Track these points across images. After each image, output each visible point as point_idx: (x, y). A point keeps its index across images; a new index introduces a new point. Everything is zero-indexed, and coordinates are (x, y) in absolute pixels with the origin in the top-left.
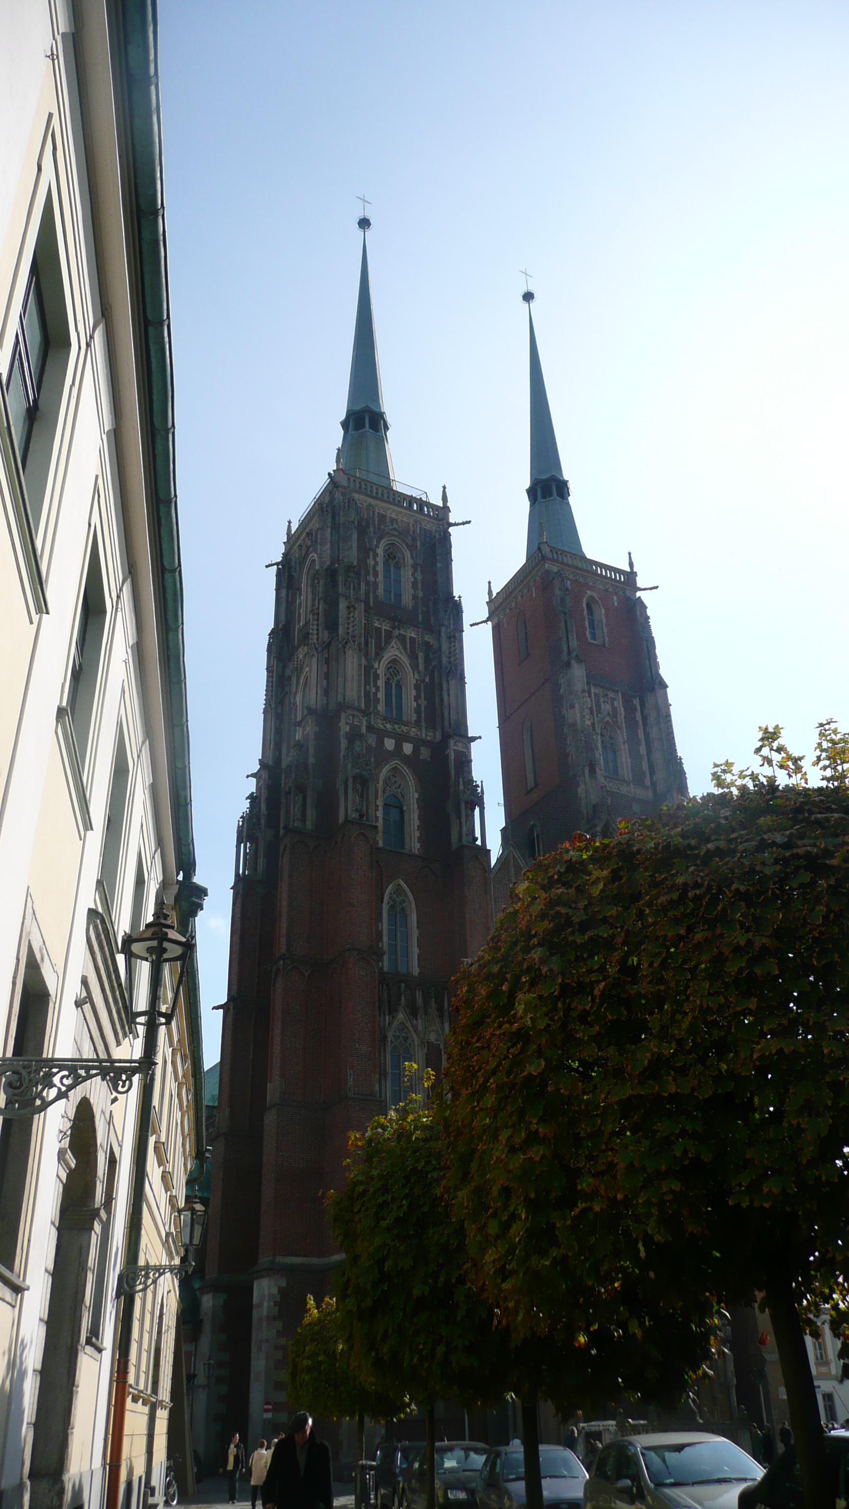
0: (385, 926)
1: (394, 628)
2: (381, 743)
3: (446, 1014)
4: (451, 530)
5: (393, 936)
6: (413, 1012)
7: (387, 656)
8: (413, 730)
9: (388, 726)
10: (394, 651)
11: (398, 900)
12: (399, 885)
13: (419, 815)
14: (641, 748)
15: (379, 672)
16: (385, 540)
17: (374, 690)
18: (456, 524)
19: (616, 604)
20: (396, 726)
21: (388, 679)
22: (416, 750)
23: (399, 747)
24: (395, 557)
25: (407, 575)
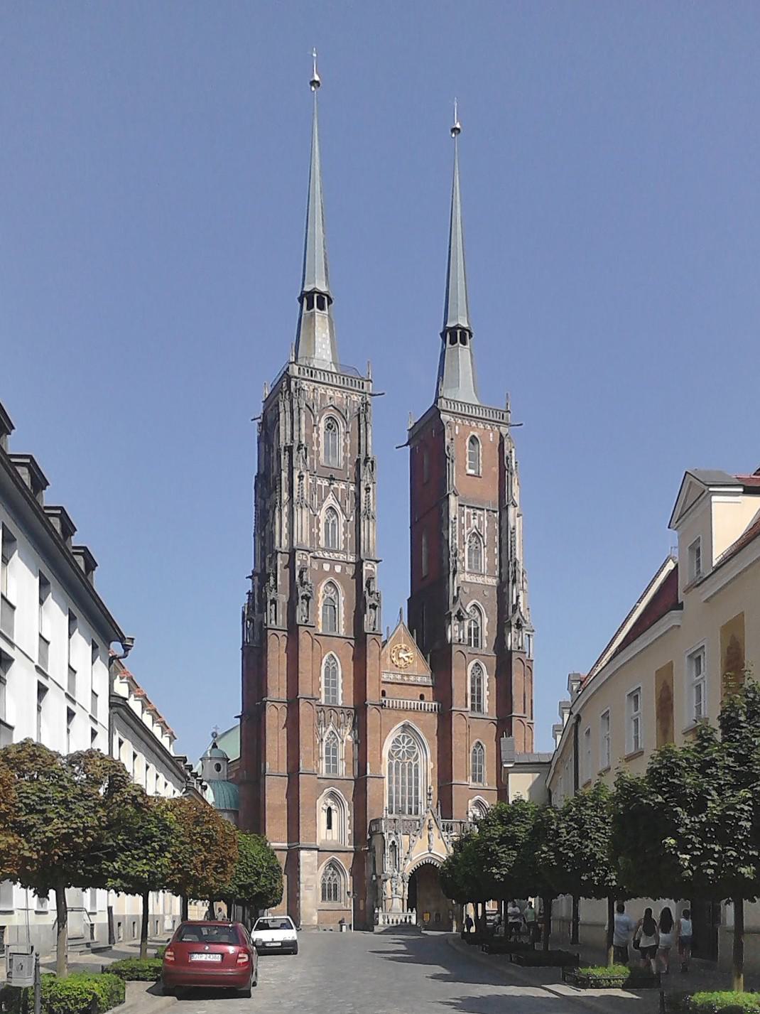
0: (322, 679)
1: (330, 484)
3: (356, 725)
5: (327, 683)
7: (325, 505)
9: (326, 554)
10: (330, 501)
11: (331, 663)
12: (331, 655)
14: (496, 549)
17: (317, 531)
19: (491, 440)
20: (331, 554)
21: (327, 520)
22: (343, 569)
23: (332, 568)
24: (332, 427)
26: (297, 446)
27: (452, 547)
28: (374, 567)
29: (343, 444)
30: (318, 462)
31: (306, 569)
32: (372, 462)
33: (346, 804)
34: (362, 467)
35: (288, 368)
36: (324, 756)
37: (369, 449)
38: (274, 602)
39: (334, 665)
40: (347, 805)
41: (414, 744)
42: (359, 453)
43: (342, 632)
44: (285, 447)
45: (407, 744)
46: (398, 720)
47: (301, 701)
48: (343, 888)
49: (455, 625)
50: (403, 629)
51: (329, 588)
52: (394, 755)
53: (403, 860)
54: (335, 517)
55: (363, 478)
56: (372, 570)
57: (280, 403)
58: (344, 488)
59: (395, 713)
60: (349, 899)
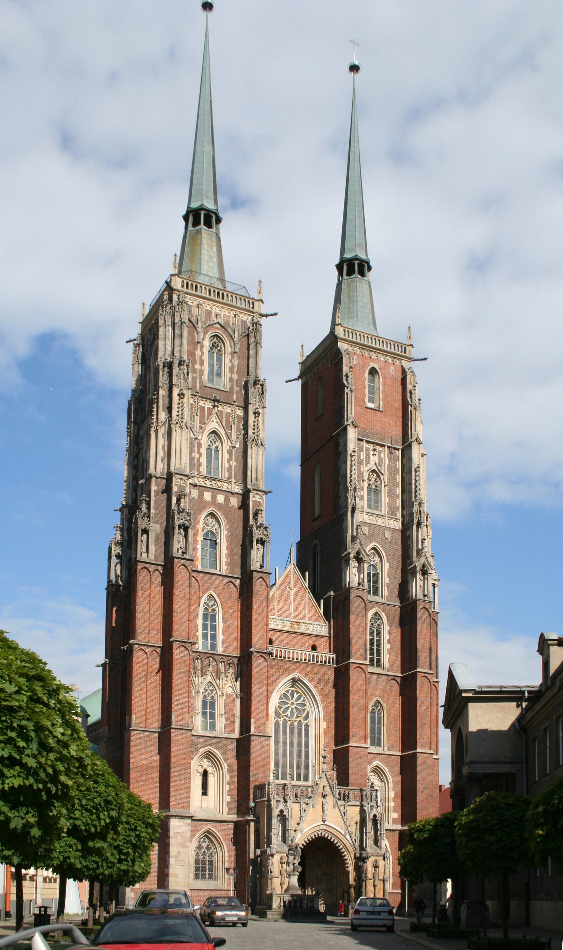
0: (200, 622)
1: (214, 407)
2: (201, 496)
4: (263, 321)
5: (205, 627)
6: (218, 674)
8: (226, 484)
9: (208, 483)
10: (213, 424)
11: (210, 604)
12: (211, 594)
13: (227, 546)
15: (201, 442)
16: (210, 333)
17: (197, 456)
18: (266, 316)
20: (213, 482)
21: (209, 446)
22: (227, 500)
23: (214, 498)
25: (227, 361)
26: (178, 362)
27: (351, 481)
28: (262, 499)
29: (230, 365)
30: (201, 382)
31: (185, 495)
32: (262, 385)
33: (225, 766)
34: (251, 390)
35: (171, 280)
36: (200, 710)
37: (259, 372)
38: (146, 531)
39: (214, 607)
40: (226, 767)
41: (304, 701)
42: (248, 374)
43: (224, 569)
44: (164, 363)
45: (295, 701)
46: (287, 671)
47: (176, 645)
48: (220, 865)
49: (354, 567)
50: (292, 569)
51: (210, 520)
52: (281, 712)
53: (293, 832)
54: (218, 443)
55: (252, 400)
56: (260, 502)
57: (160, 317)
58: (230, 411)
59: (283, 665)
60: (226, 876)
